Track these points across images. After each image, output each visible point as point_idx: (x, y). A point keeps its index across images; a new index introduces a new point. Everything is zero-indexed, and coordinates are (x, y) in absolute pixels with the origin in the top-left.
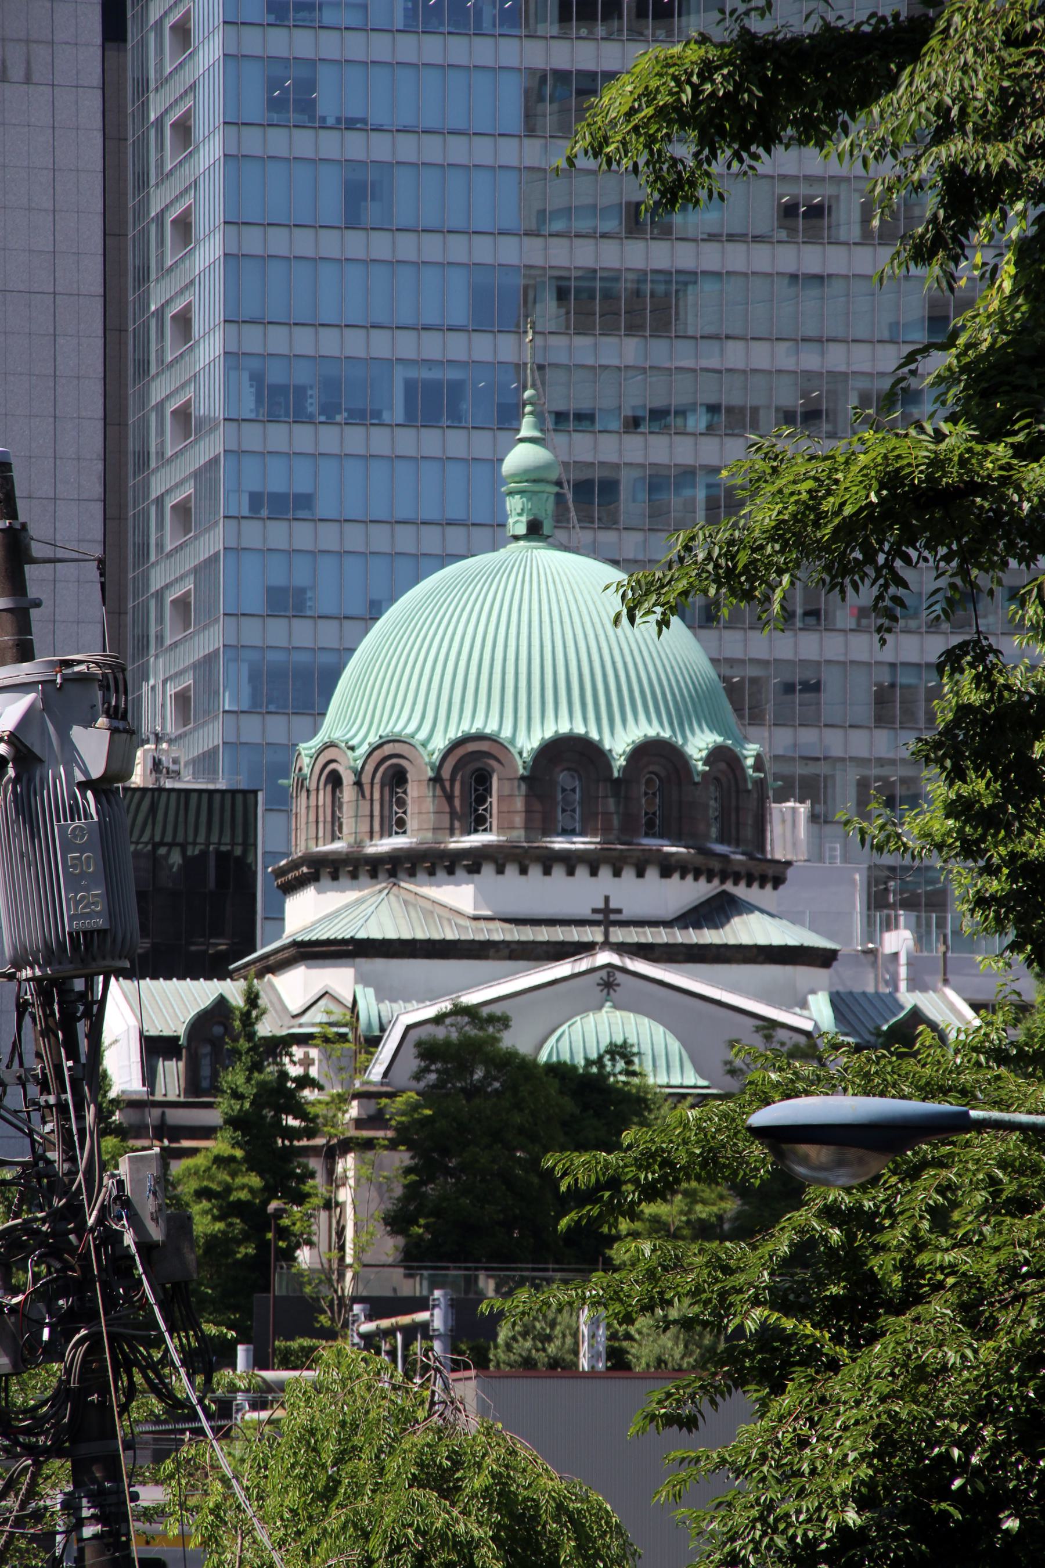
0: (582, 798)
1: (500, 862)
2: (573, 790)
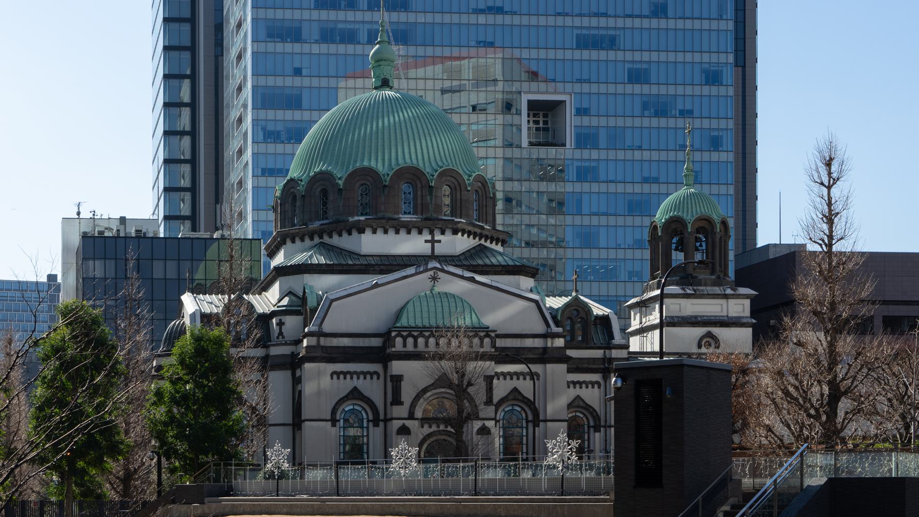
0: (414, 197)
1: (374, 227)
2: (410, 193)
